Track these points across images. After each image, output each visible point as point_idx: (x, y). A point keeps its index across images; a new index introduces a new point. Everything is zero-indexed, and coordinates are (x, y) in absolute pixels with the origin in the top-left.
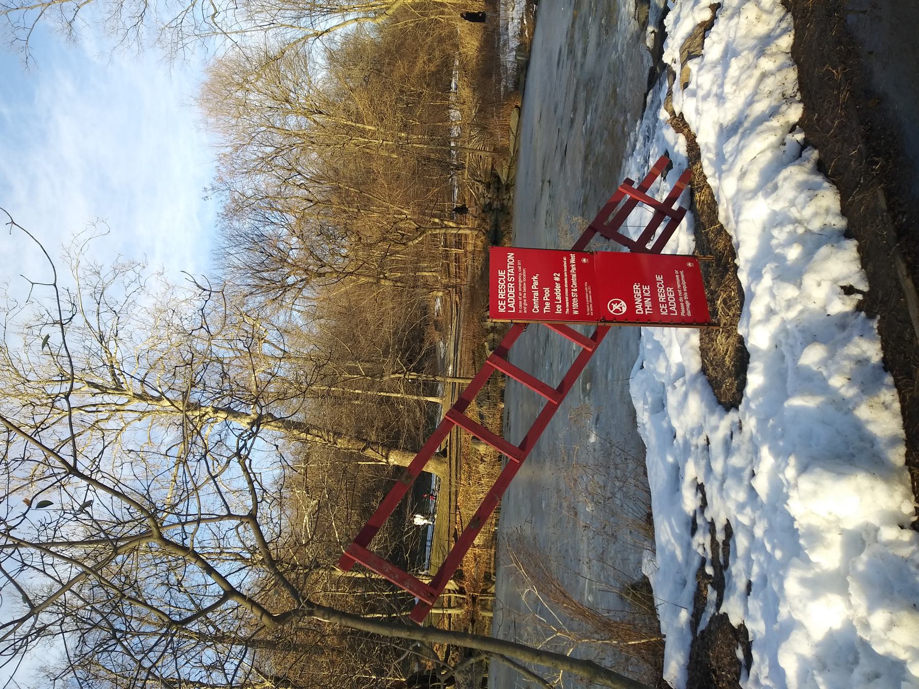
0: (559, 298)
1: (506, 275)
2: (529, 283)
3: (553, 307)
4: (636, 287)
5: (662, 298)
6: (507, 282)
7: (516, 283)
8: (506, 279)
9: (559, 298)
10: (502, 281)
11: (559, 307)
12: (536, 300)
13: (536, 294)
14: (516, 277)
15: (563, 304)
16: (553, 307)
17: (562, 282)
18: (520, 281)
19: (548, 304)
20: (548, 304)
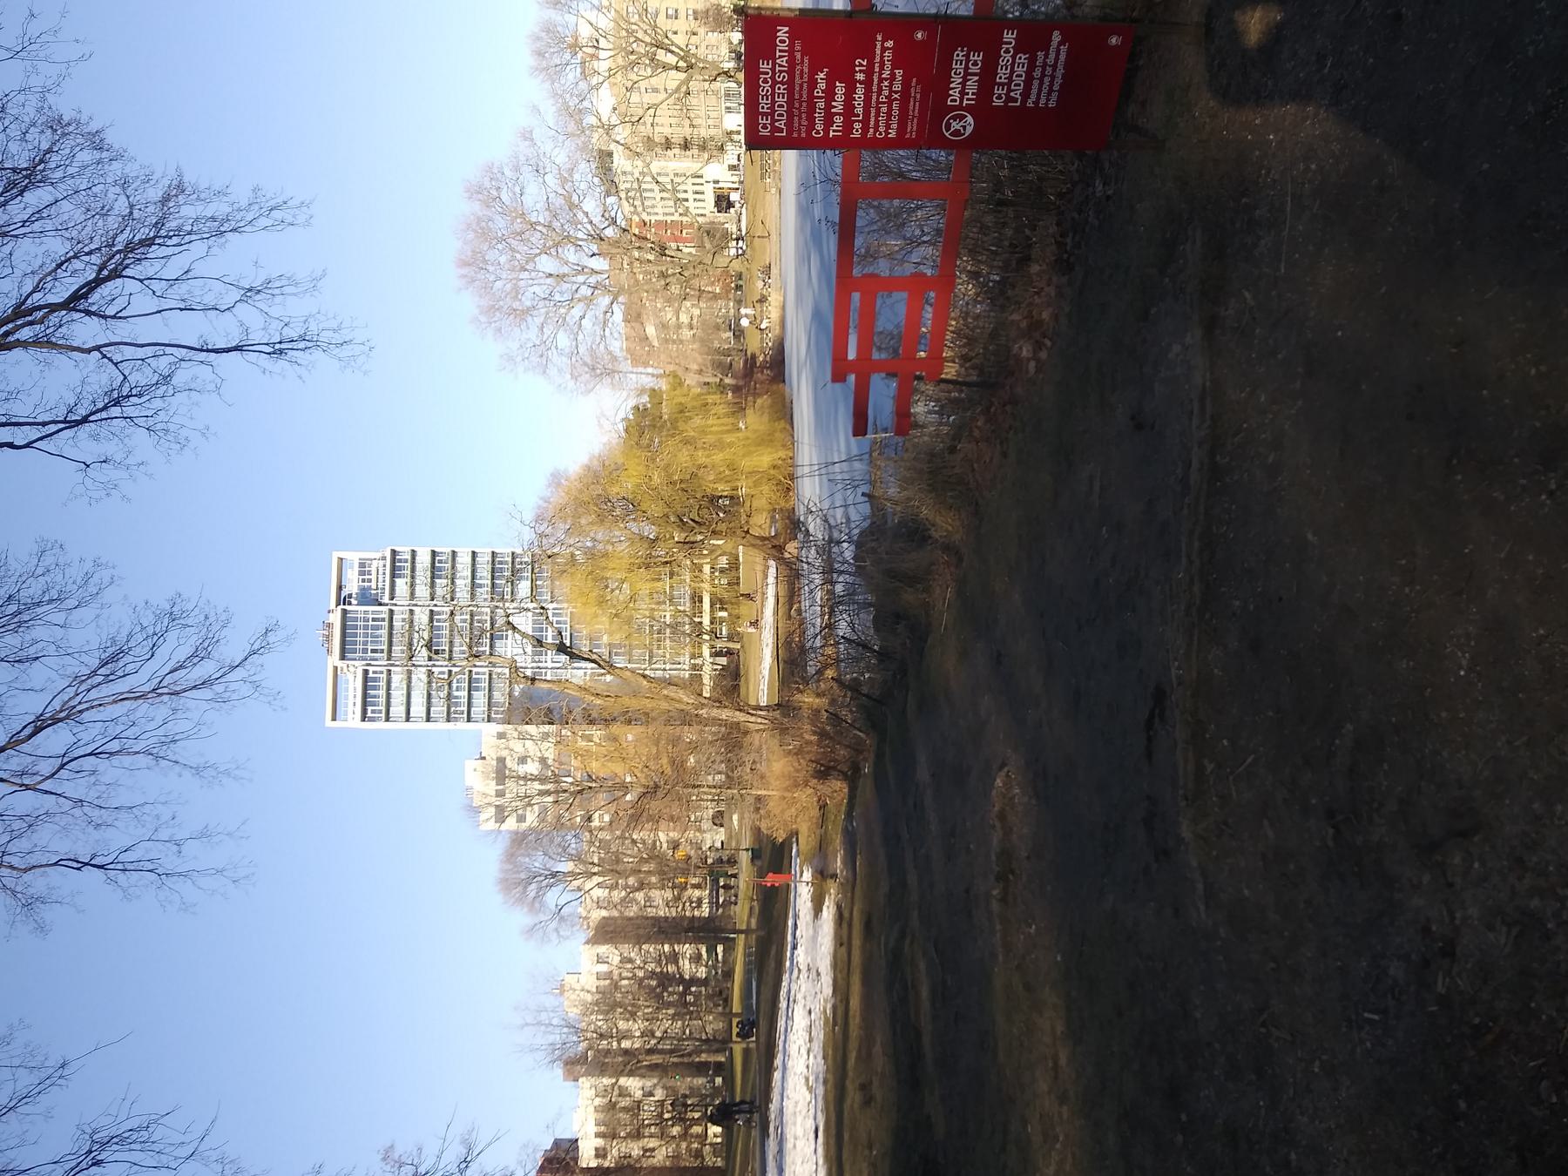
0: (859, 110)
1: (773, 69)
2: (813, 84)
3: (848, 127)
4: (959, 55)
5: (1002, 75)
6: (775, 83)
7: (790, 85)
8: (773, 78)
9: (859, 110)
10: (765, 81)
11: (857, 126)
12: (819, 116)
13: (821, 104)
14: (791, 72)
15: (865, 122)
16: (848, 127)
17: (868, 83)
18: (798, 80)
19: (838, 120)
20: (838, 120)
